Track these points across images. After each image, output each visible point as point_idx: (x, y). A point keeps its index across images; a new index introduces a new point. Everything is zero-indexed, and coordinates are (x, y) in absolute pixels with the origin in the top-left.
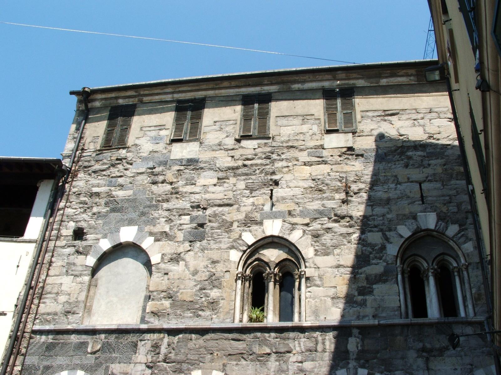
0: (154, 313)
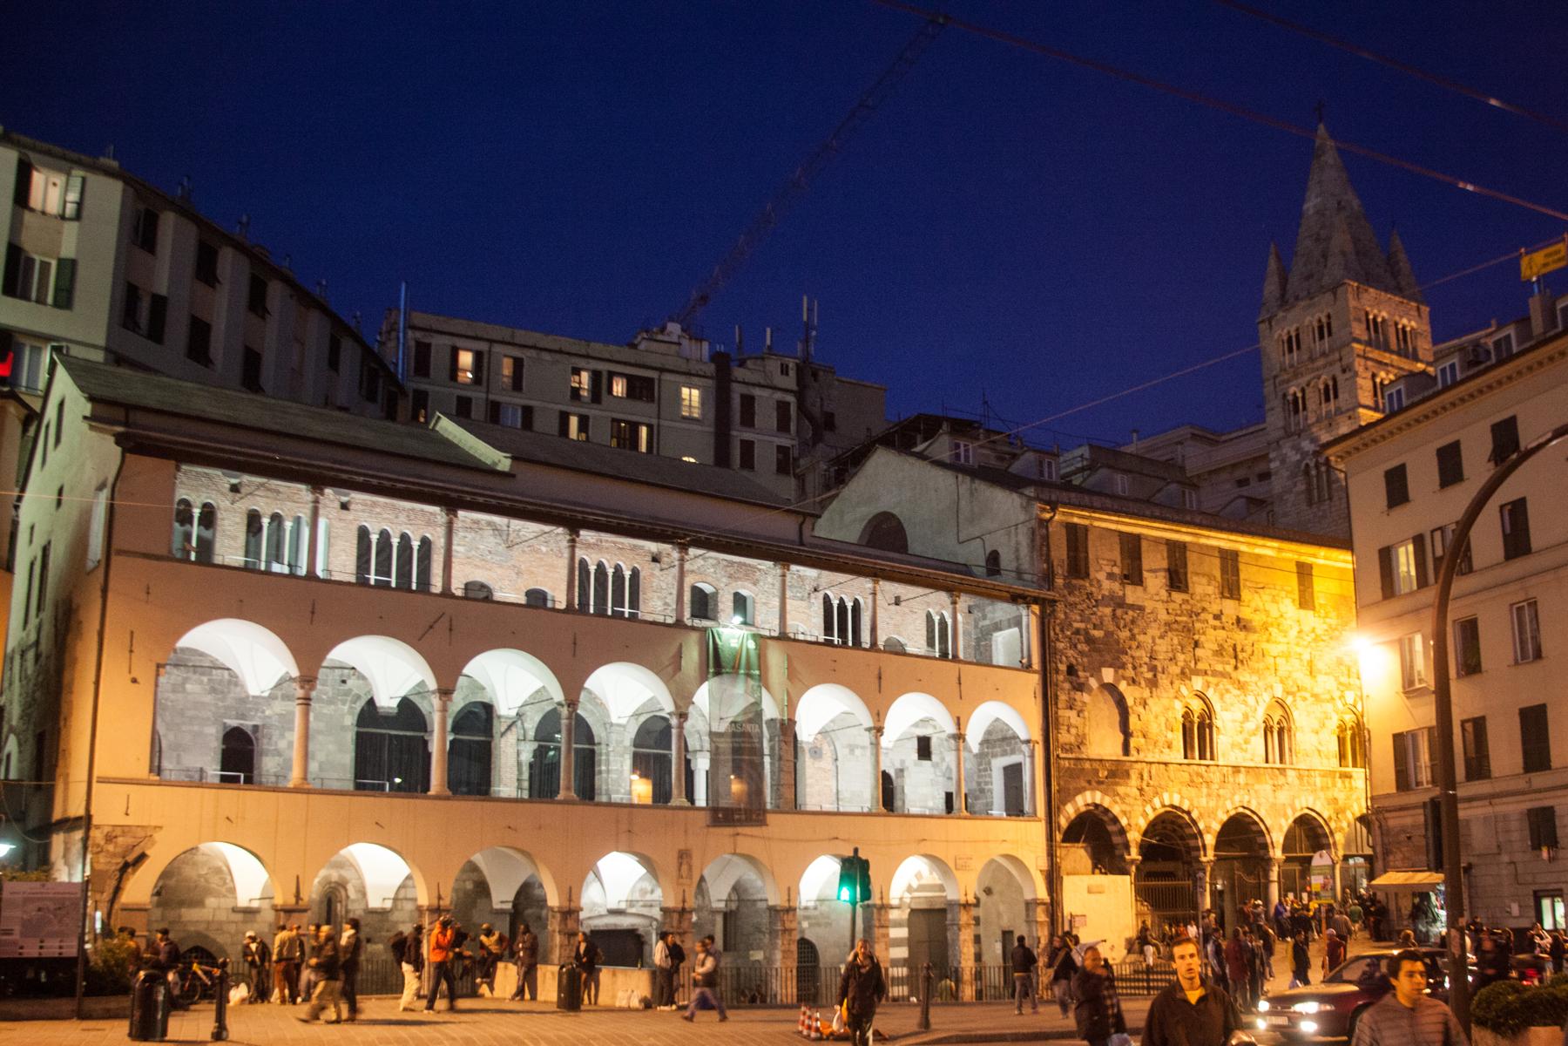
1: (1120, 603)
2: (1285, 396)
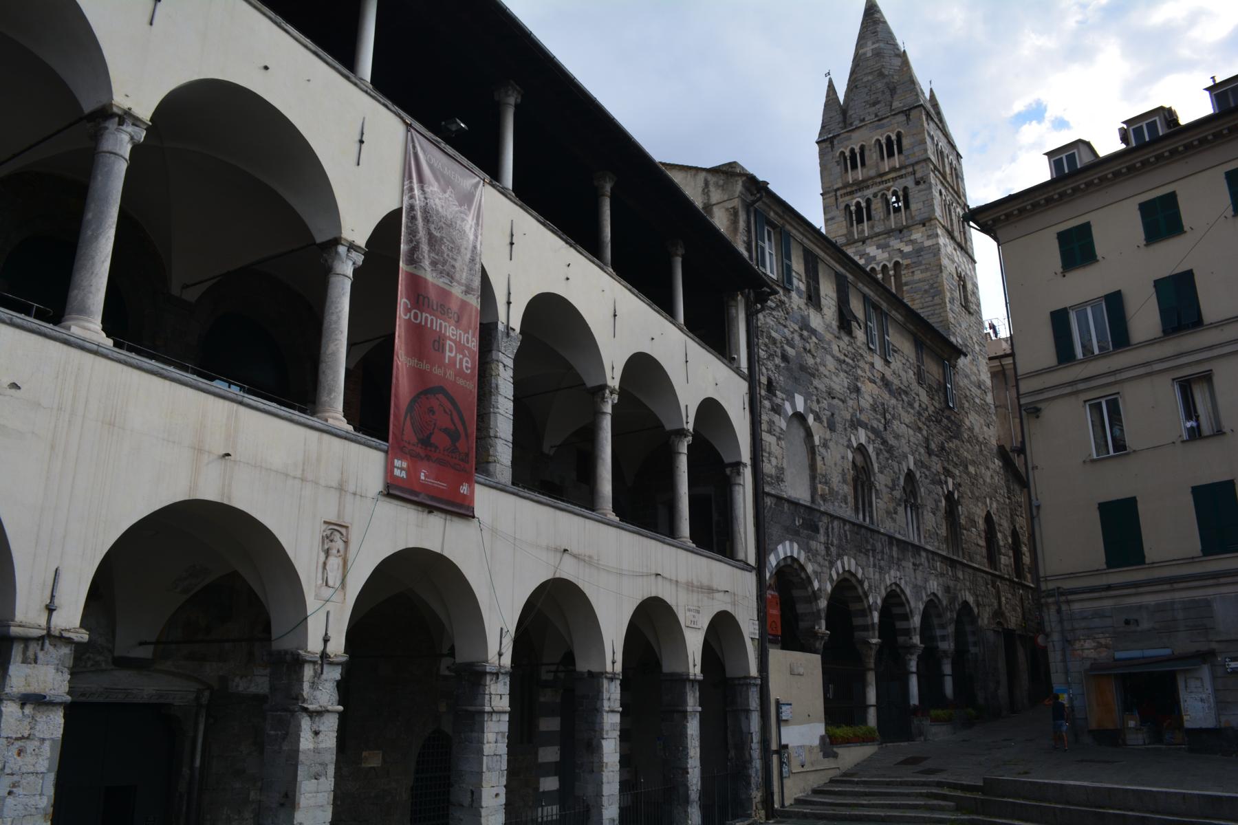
0: (822, 496)
1: (805, 325)
2: (847, 207)
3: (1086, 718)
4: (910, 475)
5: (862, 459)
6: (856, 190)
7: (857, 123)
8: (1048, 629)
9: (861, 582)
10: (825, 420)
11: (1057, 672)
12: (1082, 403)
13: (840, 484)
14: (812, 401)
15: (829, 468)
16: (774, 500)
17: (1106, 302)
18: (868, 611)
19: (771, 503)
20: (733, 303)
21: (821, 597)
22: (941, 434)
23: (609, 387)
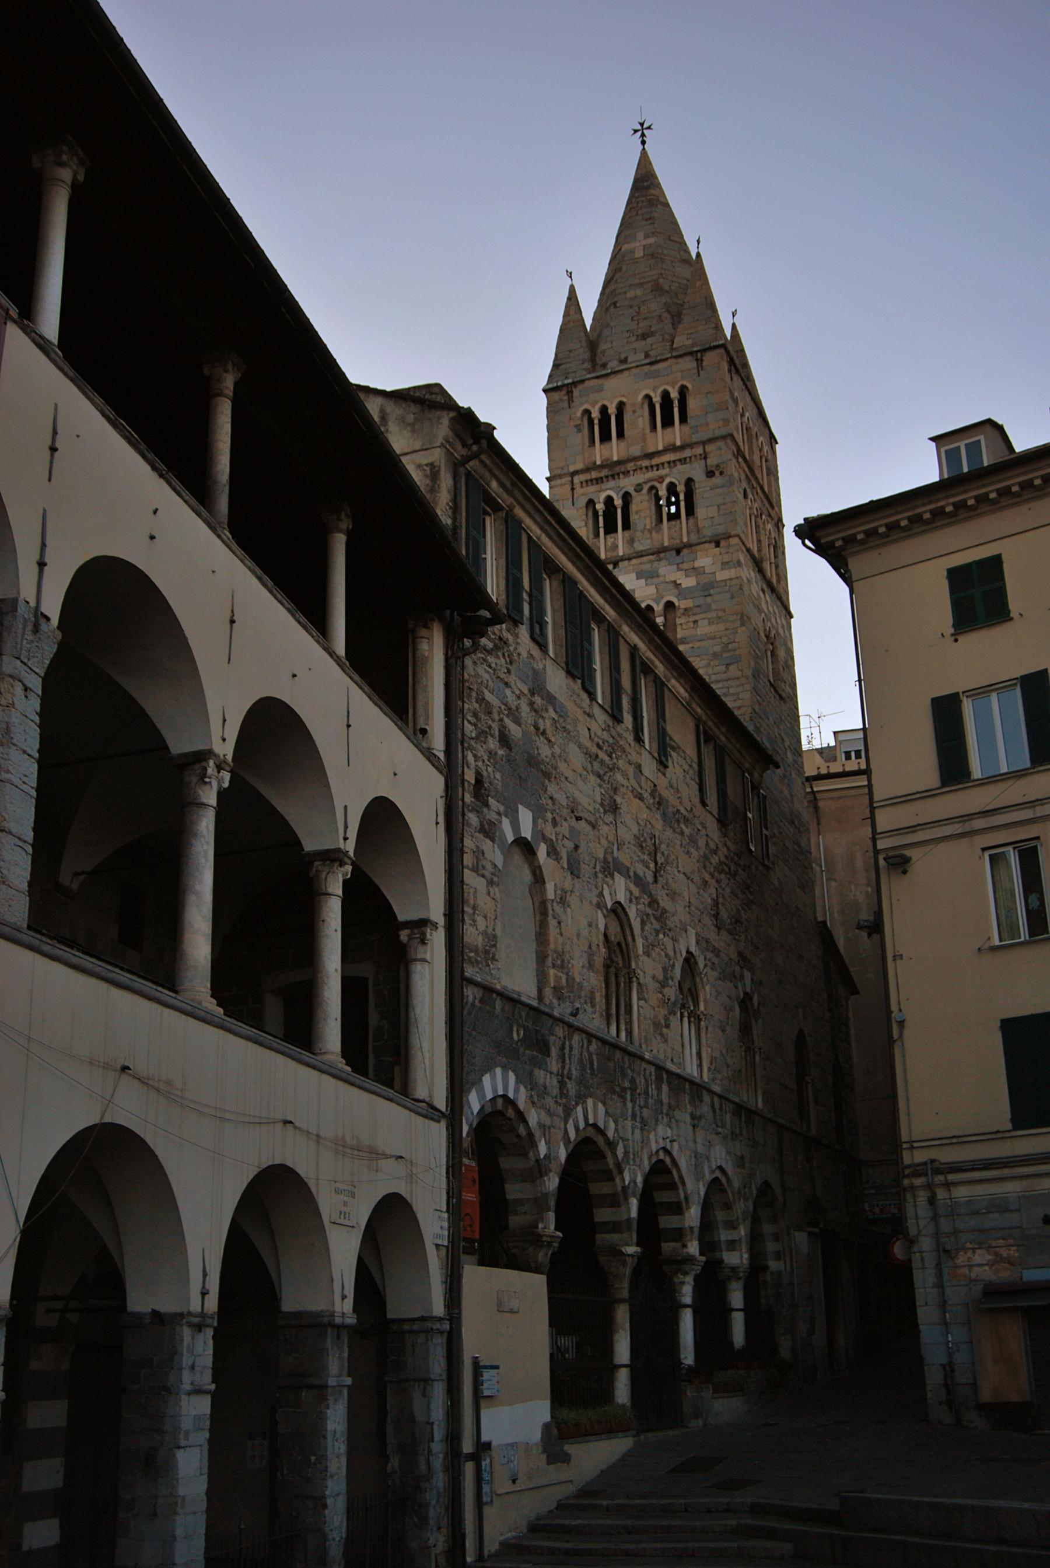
1: (538, 687)
2: (591, 503)
3: (975, 1384)
4: (690, 960)
5: (619, 930)
6: (607, 477)
7: (613, 365)
8: (913, 1231)
9: (612, 1145)
10: (564, 856)
11: (926, 1304)
12: (980, 852)
13: (585, 970)
14: (546, 821)
15: (568, 942)
16: (479, 993)
17: (1022, 687)
18: (622, 1198)
19: (475, 998)
20: (423, 632)
21: (550, 1171)
22: (736, 895)
23: (216, 756)
